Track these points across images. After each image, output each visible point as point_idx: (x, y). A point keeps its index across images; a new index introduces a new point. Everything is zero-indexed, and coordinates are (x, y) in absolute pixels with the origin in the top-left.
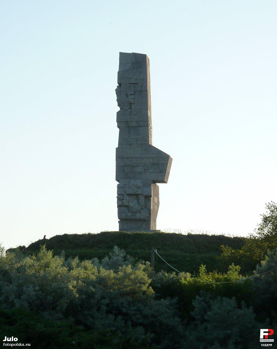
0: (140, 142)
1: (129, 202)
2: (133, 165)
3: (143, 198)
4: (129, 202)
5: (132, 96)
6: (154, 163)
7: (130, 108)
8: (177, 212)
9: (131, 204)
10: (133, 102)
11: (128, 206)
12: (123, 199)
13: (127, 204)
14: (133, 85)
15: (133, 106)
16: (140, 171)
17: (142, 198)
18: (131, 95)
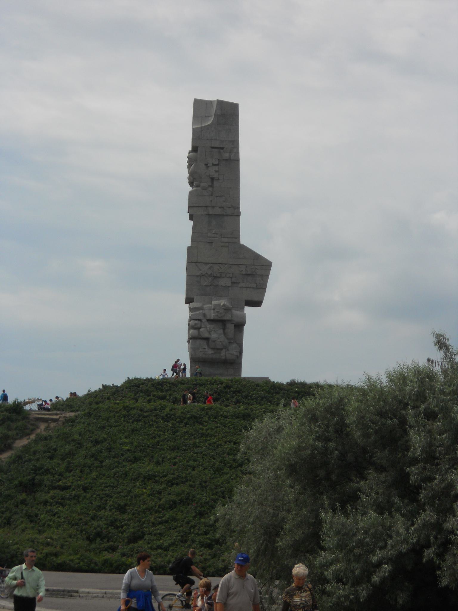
0: (226, 240)
1: (209, 332)
2: (215, 275)
3: (233, 326)
4: (209, 332)
5: (214, 167)
6: (248, 273)
7: (212, 186)
8: (270, 350)
9: (214, 336)
10: (216, 175)
11: (207, 339)
12: (201, 328)
13: (206, 335)
14: (216, 150)
15: (216, 183)
16: (224, 285)
17: (230, 327)
18: (213, 165)
